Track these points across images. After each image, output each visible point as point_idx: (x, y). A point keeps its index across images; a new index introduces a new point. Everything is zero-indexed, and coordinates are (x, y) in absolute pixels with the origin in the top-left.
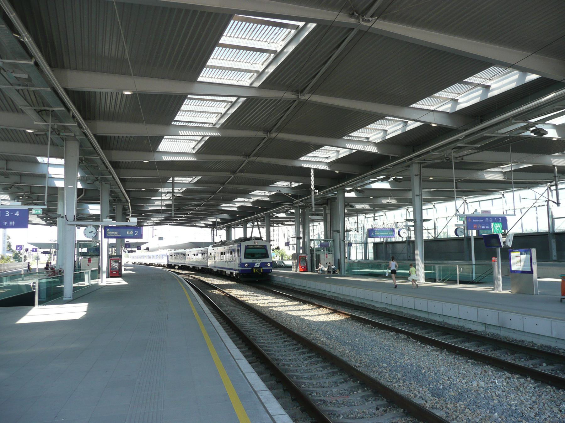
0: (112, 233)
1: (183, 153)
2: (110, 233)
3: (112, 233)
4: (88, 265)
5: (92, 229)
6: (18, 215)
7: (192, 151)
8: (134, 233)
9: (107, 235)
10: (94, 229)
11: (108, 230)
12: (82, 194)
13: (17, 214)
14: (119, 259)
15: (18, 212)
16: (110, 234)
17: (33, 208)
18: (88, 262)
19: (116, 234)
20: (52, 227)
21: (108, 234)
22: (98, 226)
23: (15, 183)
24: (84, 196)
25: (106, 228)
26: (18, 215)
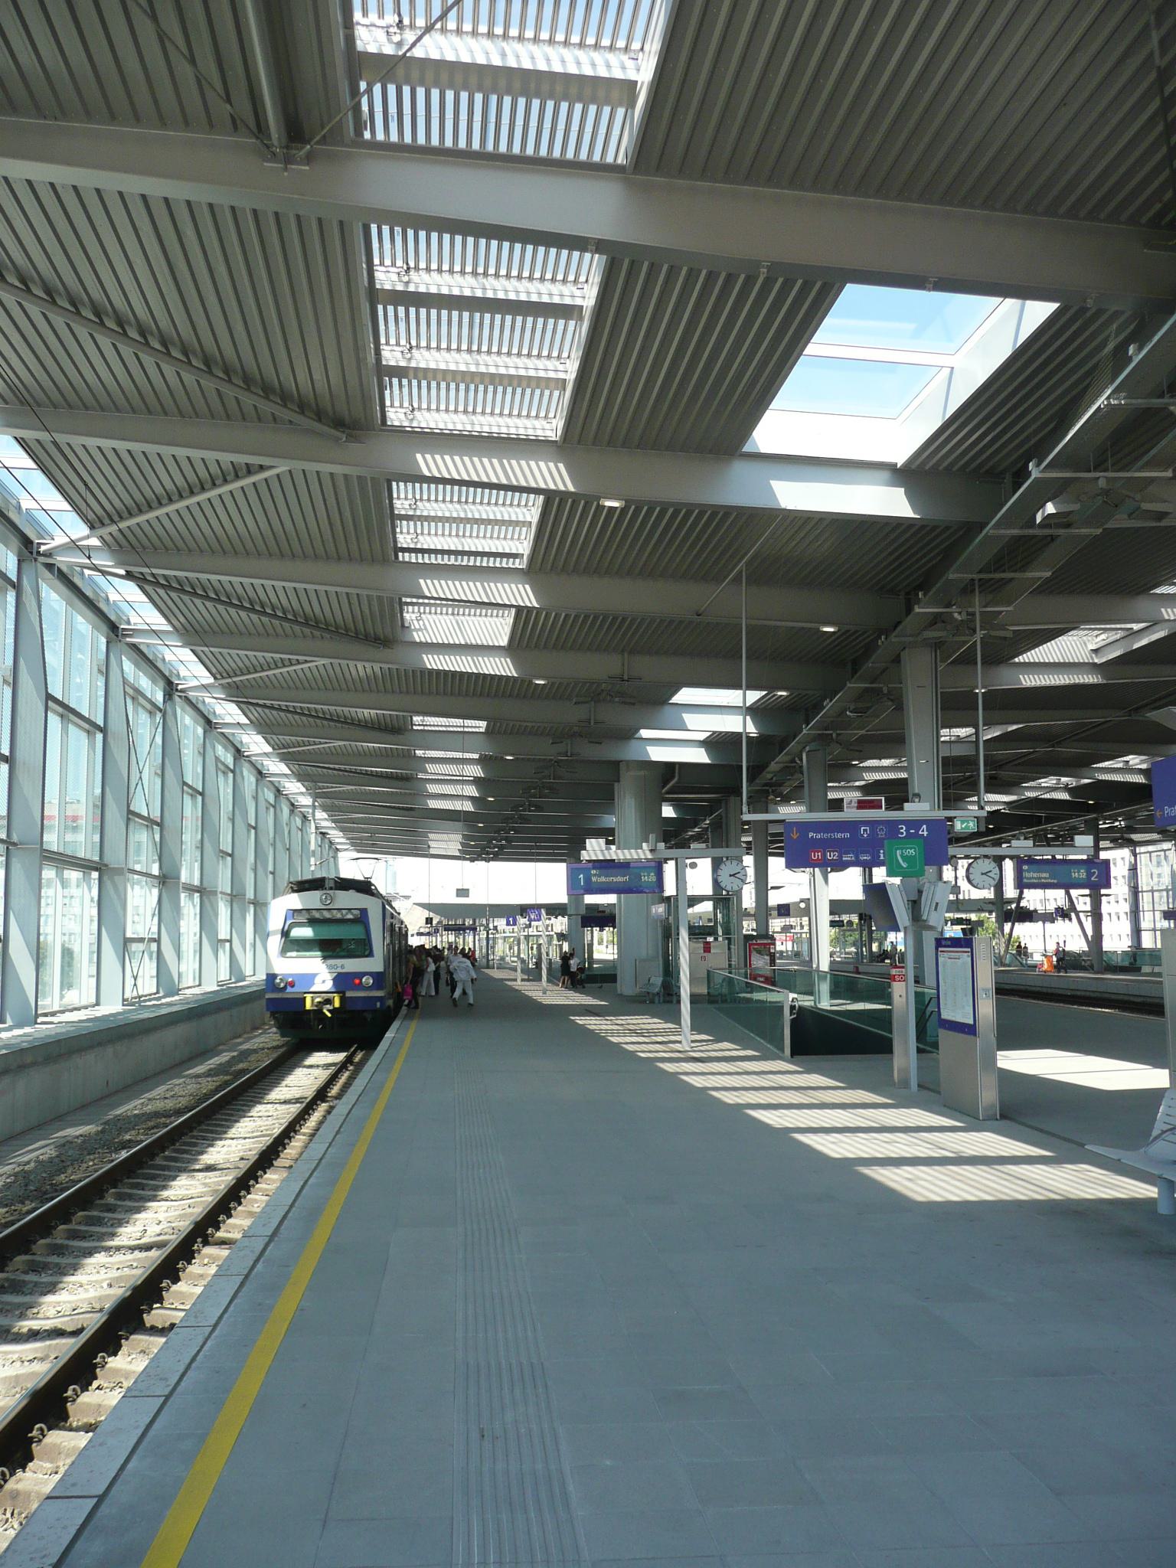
0: (1035, 875)
1: (1055, 663)
2: (1031, 874)
3: (1035, 875)
4: (703, 958)
5: (988, 865)
6: (925, 833)
7: (1093, 659)
8: (1090, 875)
9: (1025, 881)
10: (993, 865)
11: (1025, 867)
12: (673, 777)
13: (924, 831)
14: (770, 944)
15: (925, 826)
16: (1030, 878)
17: (955, 817)
18: (704, 951)
19: (1045, 878)
20: (491, 862)
21: (1028, 878)
22: (999, 860)
23: (559, 754)
24: (677, 783)
25: (1020, 862)
26: (925, 833)
